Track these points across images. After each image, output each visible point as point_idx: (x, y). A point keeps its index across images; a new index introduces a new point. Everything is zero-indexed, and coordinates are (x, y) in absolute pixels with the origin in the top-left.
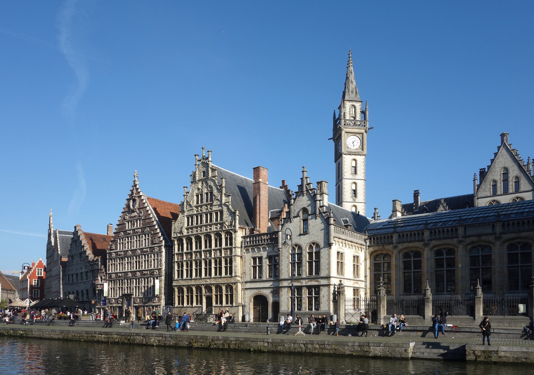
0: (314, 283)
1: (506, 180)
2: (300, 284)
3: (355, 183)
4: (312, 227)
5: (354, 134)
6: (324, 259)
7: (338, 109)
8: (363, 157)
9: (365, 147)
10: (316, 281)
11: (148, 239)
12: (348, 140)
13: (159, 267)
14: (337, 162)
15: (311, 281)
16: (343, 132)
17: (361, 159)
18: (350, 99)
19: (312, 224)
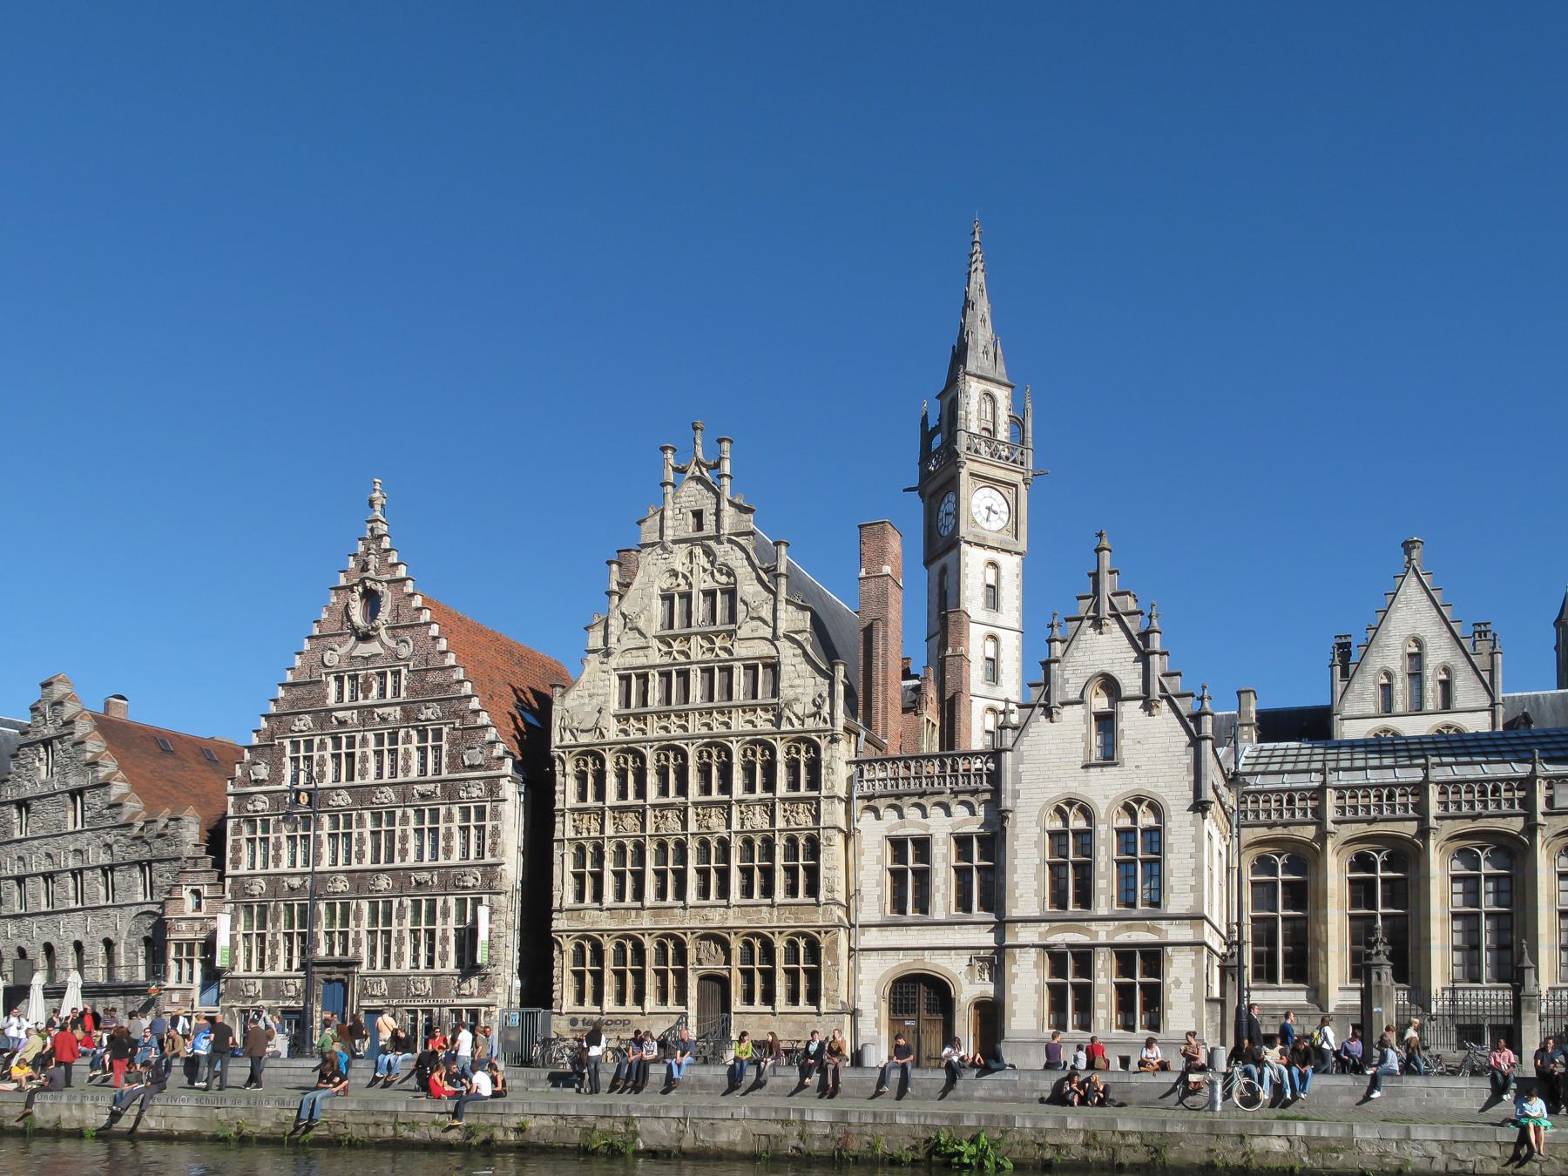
0: (1140, 936)
1: (1416, 676)
2: (1088, 938)
3: (993, 637)
4: (1130, 742)
5: (994, 482)
6: (1181, 856)
7: (937, 397)
8: (1017, 559)
9: (1023, 528)
10: (1149, 930)
11: (437, 749)
12: (975, 501)
13: (488, 859)
14: (937, 566)
15: (1129, 928)
16: (964, 473)
17: (1011, 565)
18: (979, 373)
19: (1133, 732)
